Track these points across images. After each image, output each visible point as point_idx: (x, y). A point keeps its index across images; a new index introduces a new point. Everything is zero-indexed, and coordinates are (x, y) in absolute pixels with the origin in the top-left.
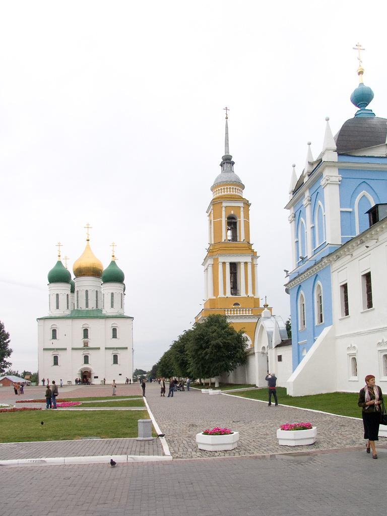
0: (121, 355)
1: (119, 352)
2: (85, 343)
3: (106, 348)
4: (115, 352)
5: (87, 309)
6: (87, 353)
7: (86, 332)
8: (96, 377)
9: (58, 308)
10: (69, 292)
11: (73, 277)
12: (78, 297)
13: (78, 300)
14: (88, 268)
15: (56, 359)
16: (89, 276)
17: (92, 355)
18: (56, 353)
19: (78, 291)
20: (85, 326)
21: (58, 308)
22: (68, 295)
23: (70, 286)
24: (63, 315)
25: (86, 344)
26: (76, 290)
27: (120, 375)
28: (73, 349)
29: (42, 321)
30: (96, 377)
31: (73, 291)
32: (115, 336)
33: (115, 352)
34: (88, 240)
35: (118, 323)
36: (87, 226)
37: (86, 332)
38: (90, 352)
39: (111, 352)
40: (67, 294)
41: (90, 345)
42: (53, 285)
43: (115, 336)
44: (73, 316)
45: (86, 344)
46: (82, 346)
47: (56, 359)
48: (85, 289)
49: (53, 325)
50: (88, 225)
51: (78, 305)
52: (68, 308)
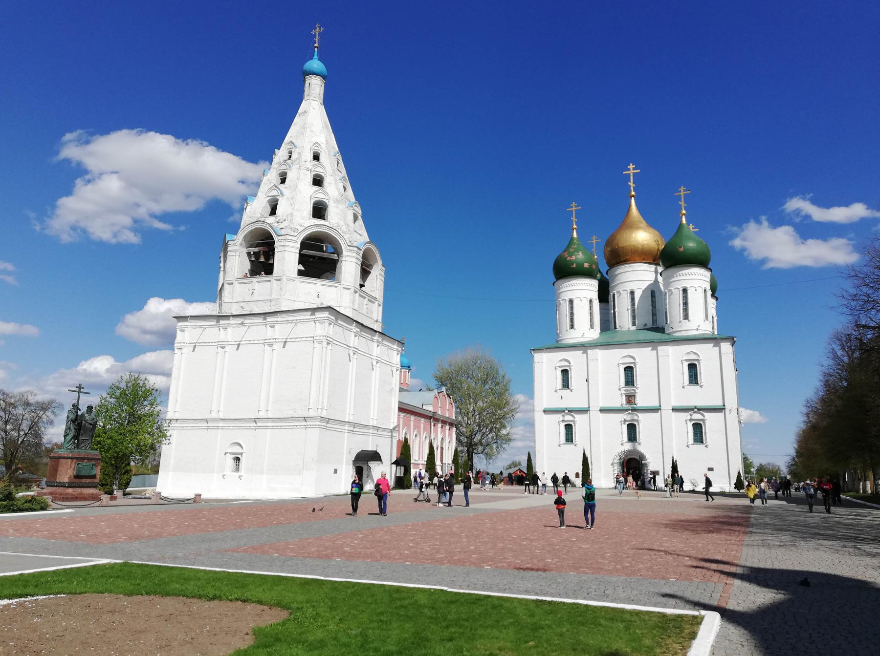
0: (712, 422)
4: (697, 416)
5: (634, 328)
7: (629, 371)
9: (572, 327)
10: (595, 296)
15: (569, 428)
17: (644, 422)
19: (614, 295)
25: (630, 398)
31: (605, 294)
32: (694, 379)
33: (697, 416)
35: (706, 354)
37: (629, 371)
38: (641, 416)
39: (686, 416)
41: (640, 402)
43: (694, 379)
45: (630, 398)
46: (620, 401)
47: (569, 428)
49: (561, 360)
52: (592, 326)
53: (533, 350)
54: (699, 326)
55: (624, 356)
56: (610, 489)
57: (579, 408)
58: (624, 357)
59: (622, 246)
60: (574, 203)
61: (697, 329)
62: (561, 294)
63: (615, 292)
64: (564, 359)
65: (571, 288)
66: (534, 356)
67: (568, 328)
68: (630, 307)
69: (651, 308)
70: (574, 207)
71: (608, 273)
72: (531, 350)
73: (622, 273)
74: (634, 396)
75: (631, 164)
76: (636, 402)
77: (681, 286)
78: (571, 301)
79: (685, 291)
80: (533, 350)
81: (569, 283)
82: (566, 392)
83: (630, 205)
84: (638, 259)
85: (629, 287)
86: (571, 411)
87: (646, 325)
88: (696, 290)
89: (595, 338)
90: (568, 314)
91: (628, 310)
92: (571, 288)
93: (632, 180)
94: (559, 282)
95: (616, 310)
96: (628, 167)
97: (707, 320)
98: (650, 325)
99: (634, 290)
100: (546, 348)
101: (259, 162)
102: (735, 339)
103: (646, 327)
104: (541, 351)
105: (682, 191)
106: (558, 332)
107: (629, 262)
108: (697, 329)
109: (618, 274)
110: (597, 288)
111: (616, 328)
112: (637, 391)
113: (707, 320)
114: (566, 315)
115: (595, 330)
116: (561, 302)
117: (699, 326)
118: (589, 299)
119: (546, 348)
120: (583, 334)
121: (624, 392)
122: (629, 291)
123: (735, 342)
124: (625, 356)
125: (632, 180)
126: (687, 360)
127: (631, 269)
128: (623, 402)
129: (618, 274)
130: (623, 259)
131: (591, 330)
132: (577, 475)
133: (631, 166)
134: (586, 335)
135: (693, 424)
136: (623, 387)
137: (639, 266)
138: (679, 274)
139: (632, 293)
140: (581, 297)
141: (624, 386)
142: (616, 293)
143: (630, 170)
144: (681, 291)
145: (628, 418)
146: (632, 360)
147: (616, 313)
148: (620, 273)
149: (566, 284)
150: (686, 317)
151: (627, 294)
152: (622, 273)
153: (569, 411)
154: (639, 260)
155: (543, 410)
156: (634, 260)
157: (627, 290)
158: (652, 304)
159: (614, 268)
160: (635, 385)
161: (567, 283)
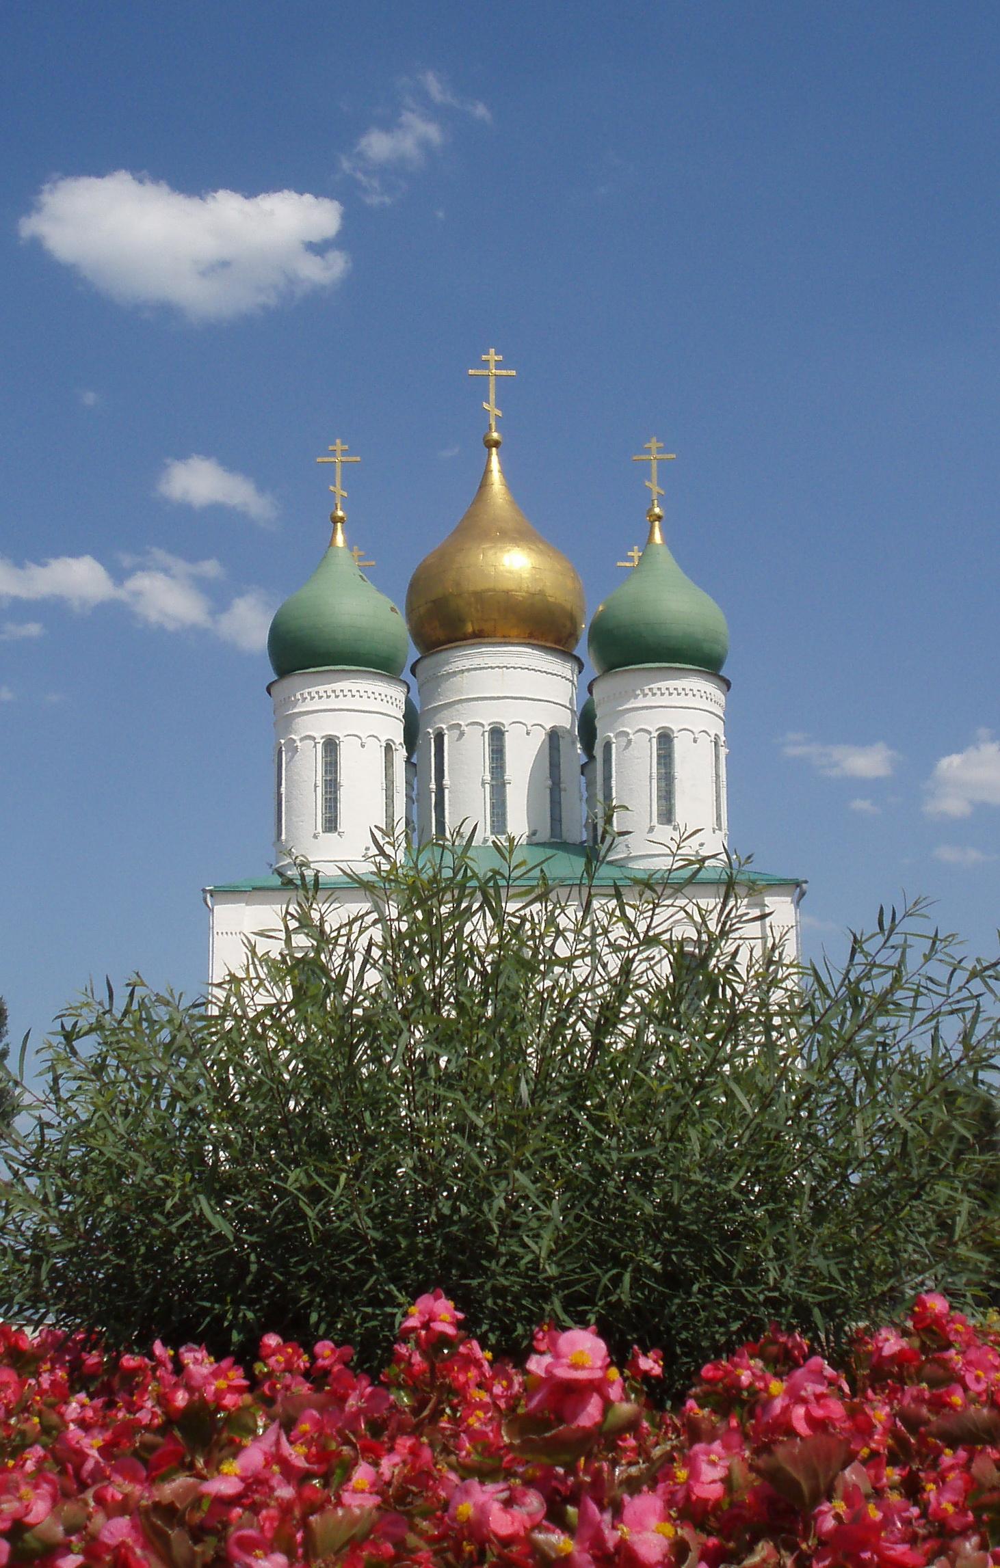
9: (331, 824)
10: (397, 733)
14: (507, 592)
19: (440, 737)
22: (389, 748)
40: (383, 738)
48: (487, 722)
53: (212, 893)
54: (702, 845)
59: (471, 589)
60: (338, 441)
62: (299, 720)
63: (444, 726)
65: (333, 703)
66: (212, 910)
67: (320, 829)
68: (488, 777)
69: (549, 782)
70: (338, 453)
72: (204, 891)
73: (469, 670)
75: (492, 351)
77: (655, 722)
78: (331, 745)
79: (665, 739)
80: (211, 891)
81: (328, 687)
83: (487, 471)
84: (515, 632)
85: (488, 715)
90: (319, 783)
91: (483, 784)
92: (333, 703)
93: (492, 396)
94: (294, 680)
95: (446, 781)
96: (484, 357)
97: (720, 829)
100: (255, 889)
101: (161, 182)
102: (804, 885)
104: (237, 896)
105: (654, 452)
106: (283, 837)
107: (490, 640)
109: (455, 674)
110: (403, 707)
113: (720, 829)
114: (316, 786)
116: (298, 743)
117: (702, 845)
119: (255, 889)
122: (487, 728)
123: (803, 894)
125: (492, 396)
129: (455, 674)
130: (469, 628)
133: (492, 356)
137: (519, 655)
138: (650, 689)
139: (497, 734)
142: (446, 731)
143: (487, 368)
144: (654, 741)
147: (446, 791)
148: (462, 671)
149: (316, 689)
151: (483, 735)
152: (469, 670)
154: (517, 637)
156: (504, 637)
158: (551, 773)
159: (443, 656)
161: (321, 688)
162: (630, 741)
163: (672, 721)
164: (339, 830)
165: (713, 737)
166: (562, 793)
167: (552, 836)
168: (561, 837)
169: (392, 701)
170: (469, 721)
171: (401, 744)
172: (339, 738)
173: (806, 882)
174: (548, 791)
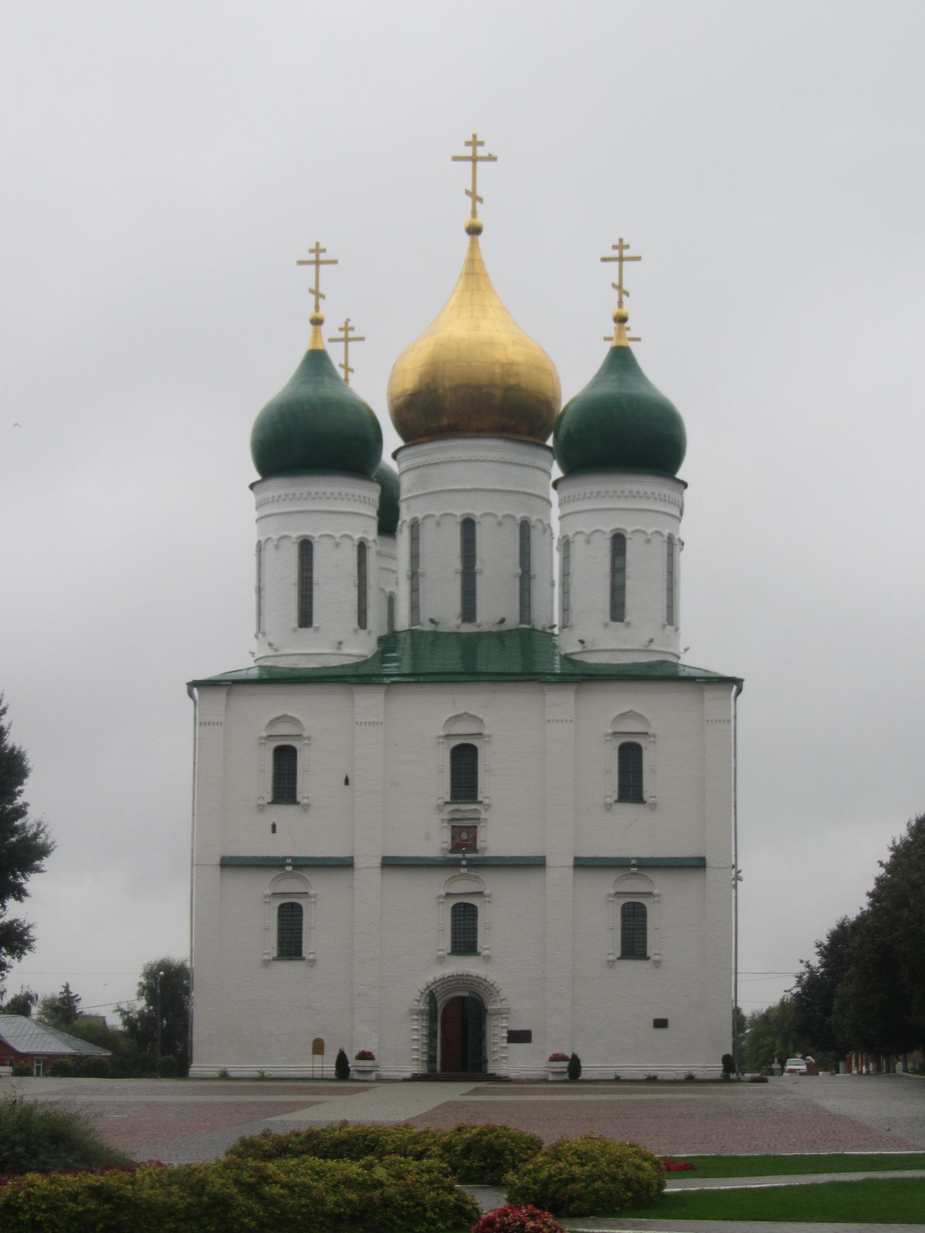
1: (660, 883)
2: (456, 831)
3: (582, 864)
6: (473, 887)
8: (520, 1037)
9: (306, 619)
10: (368, 529)
11: (391, 440)
12: (415, 557)
13: (414, 576)
16: (479, 432)
18: (290, 885)
19: (415, 526)
20: (459, 728)
21: (306, 619)
22: (362, 547)
23: (372, 493)
24: (334, 662)
26: (405, 516)
27: (661, 1024)
28: (390, 864)
29: (218, 698)
30: (520, 1037)
34: (474, 231)
36: (468, 152)
40: (357, 536)
42: (279, 487)
44: (391, 668)
50: (475, 143)
51: (415, 607)
52: (362, 622)
54: (651, 641)
55: (451, 715)
56: (405, 1080)
57: (324, 859)
58: (451, 718)
61: (646, 651)
64: (285, 716)
69: (519, 571)
71: (399, 456)
74: (475, 827)
76: (479, 845)
79: (619, 542)
82: (284, 814)
86: (303, 864)
87: (502, 621)
88: (648, 541)
89: (370, 656)
98: (513, 621)
99: (475, 516)
103: (504, 627)
108: (646, 651)
110: (377, 505)
111: (419, 623)
112: (483, 816)
115: (370, 633)
117: (651, 641)
118: (357, 543)
120: (340, 643)
121: (448, 817)
122: (459, 520)
123: (739, 691)
124: (457, 718)
126: (616, 734)
127: (465, 455)
128: (445, 845)
130: (445, 422)
131: (363, 632)
132: (318, 1047)
134: (346, 650)
135: (624, 907)
136: (447, 803)
139: (468, 526)
140: (338, 535)
141: (448, 799)
145: (462, 886)
146: (471, 728)
150: (617, 611)
153: (296, 867)
155: (217, 860)
157: (454, 516)
160: (480, 798)
162: (588, 542)
163: (628, 527)
164: (315, 624)
165: (665, 539)
166: (533, 582)
167: (522, 622)
168: (529, 623)
169: (364, 501)
170: (442, 512)
171: (374, 541)
172: (313, 538)
173: (742, 680)
174: (517, 582)
